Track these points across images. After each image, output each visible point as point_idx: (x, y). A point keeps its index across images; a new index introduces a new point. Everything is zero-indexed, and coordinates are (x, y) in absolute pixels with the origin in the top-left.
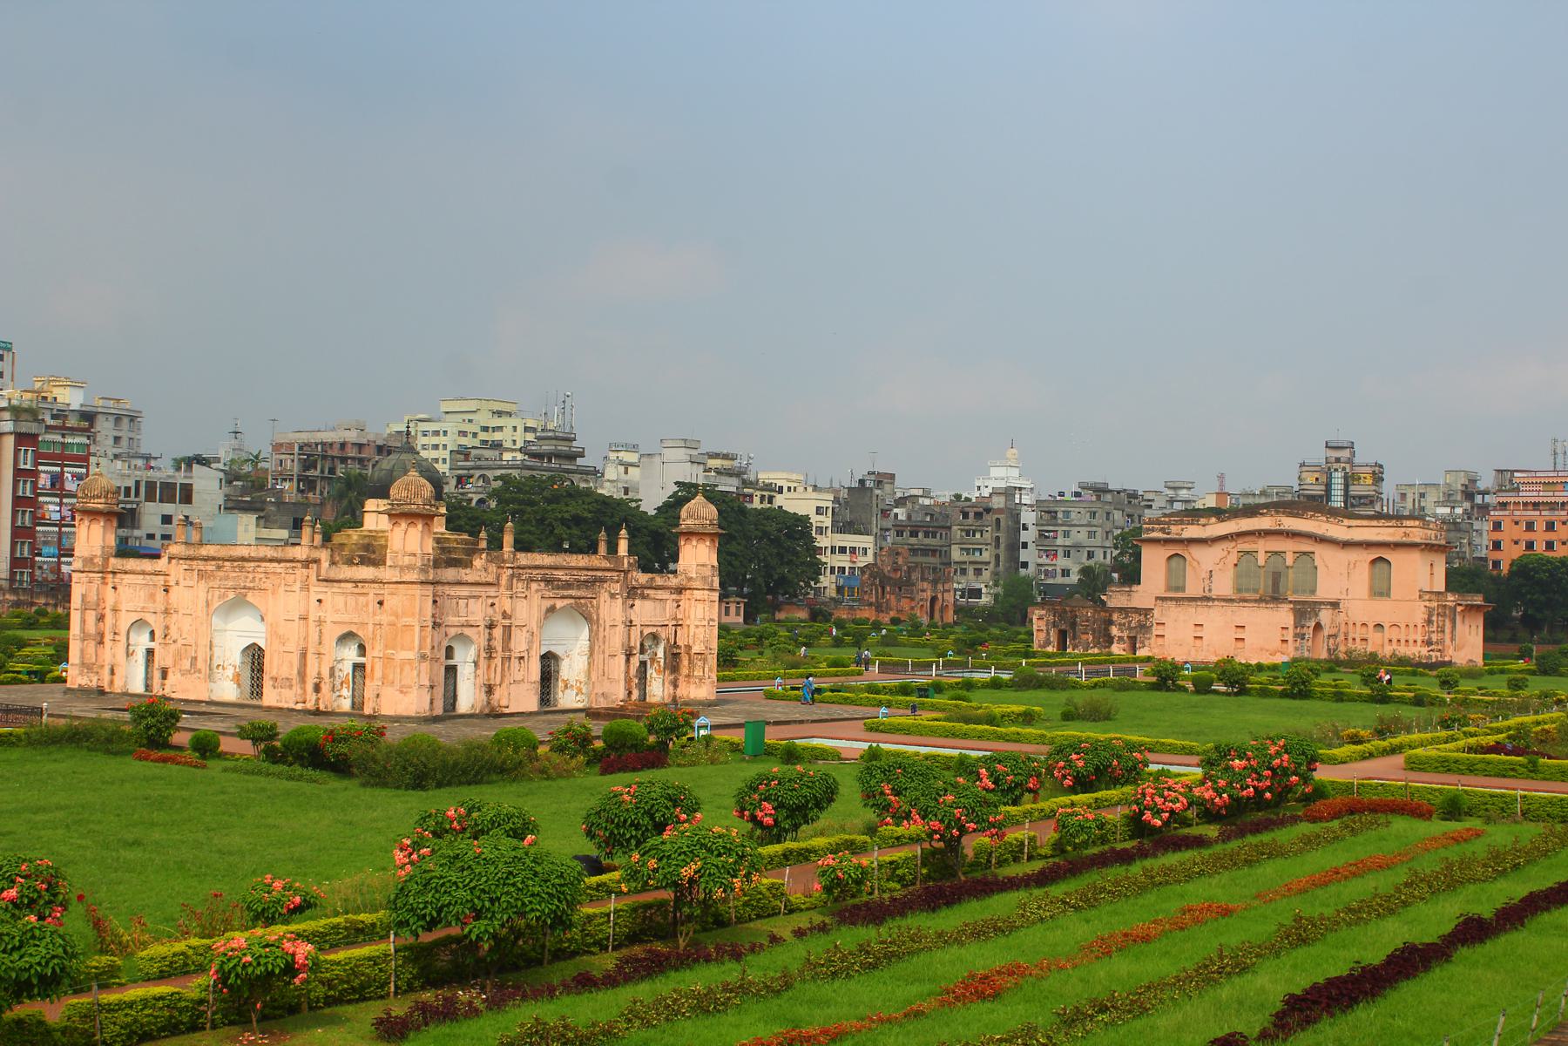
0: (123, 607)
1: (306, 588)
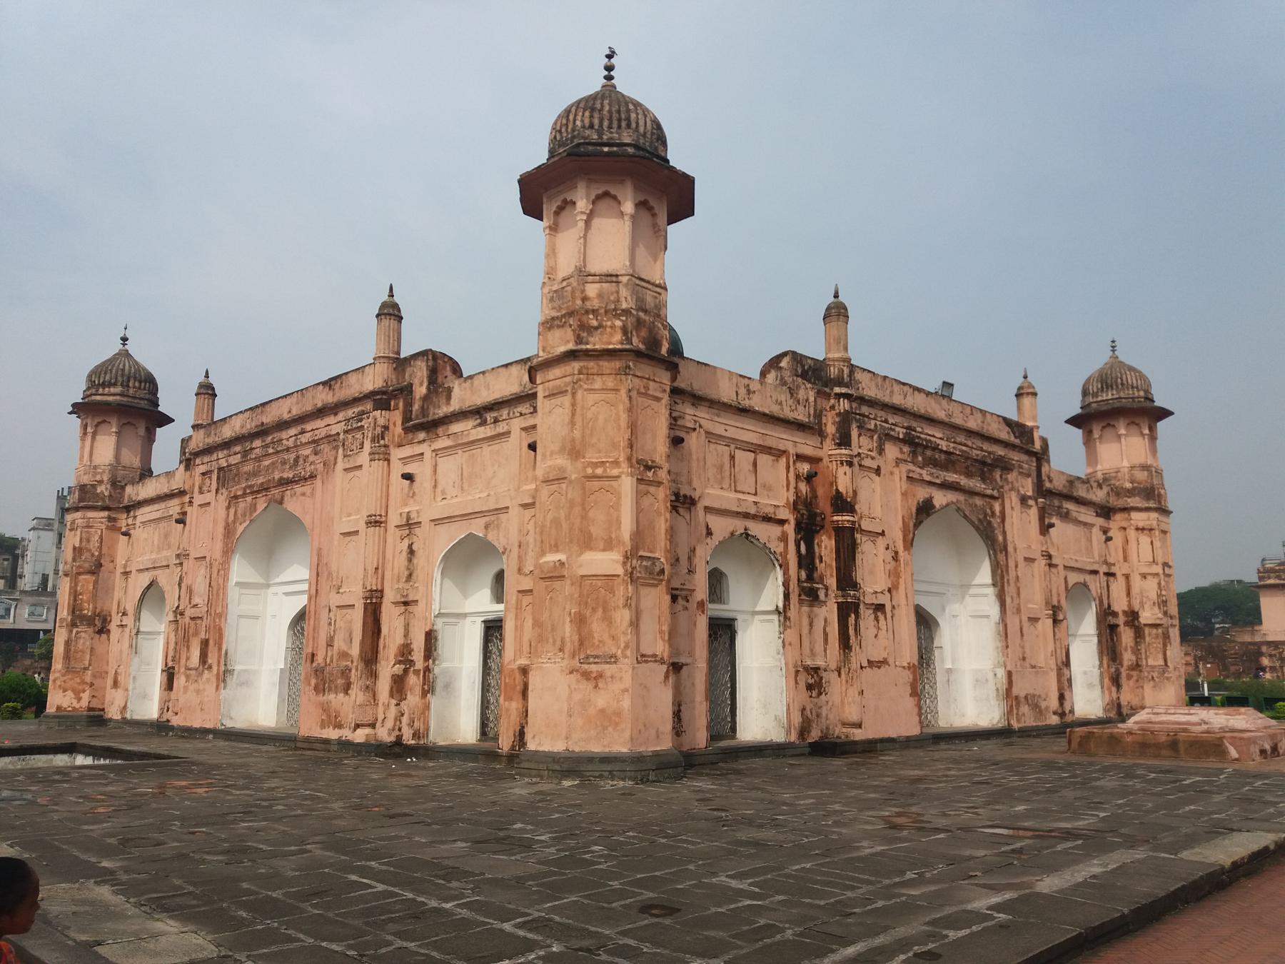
0: (133, 568)
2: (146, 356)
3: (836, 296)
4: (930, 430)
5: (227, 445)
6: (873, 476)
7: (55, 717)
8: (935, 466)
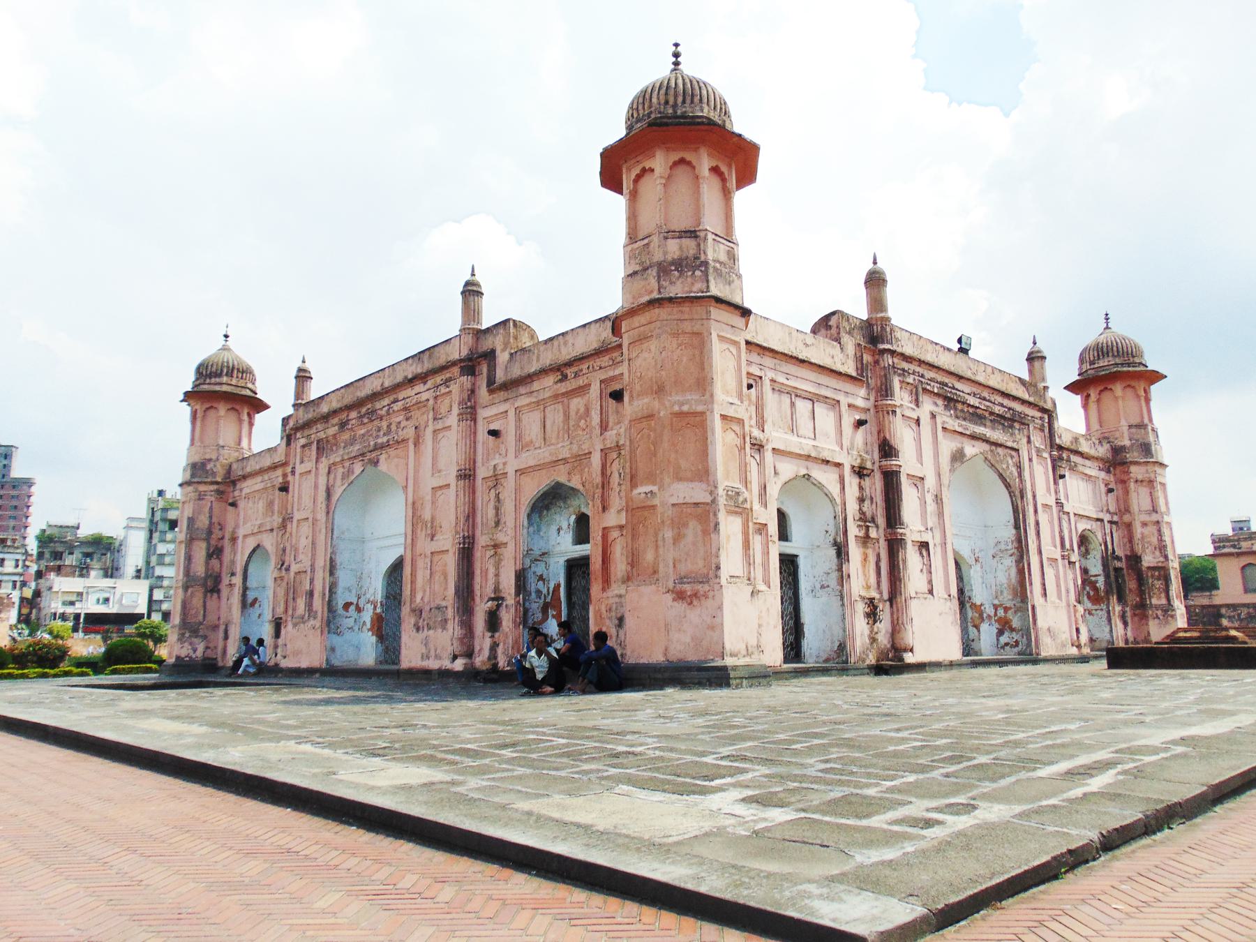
0: (241, 532)
1: (470, 412)
2: (243, 352)
3: (875, 263)
4: (959, 385)
5: (326, 418)
6: (914, 426)
7: (174, 665)
8: (965, 419)
